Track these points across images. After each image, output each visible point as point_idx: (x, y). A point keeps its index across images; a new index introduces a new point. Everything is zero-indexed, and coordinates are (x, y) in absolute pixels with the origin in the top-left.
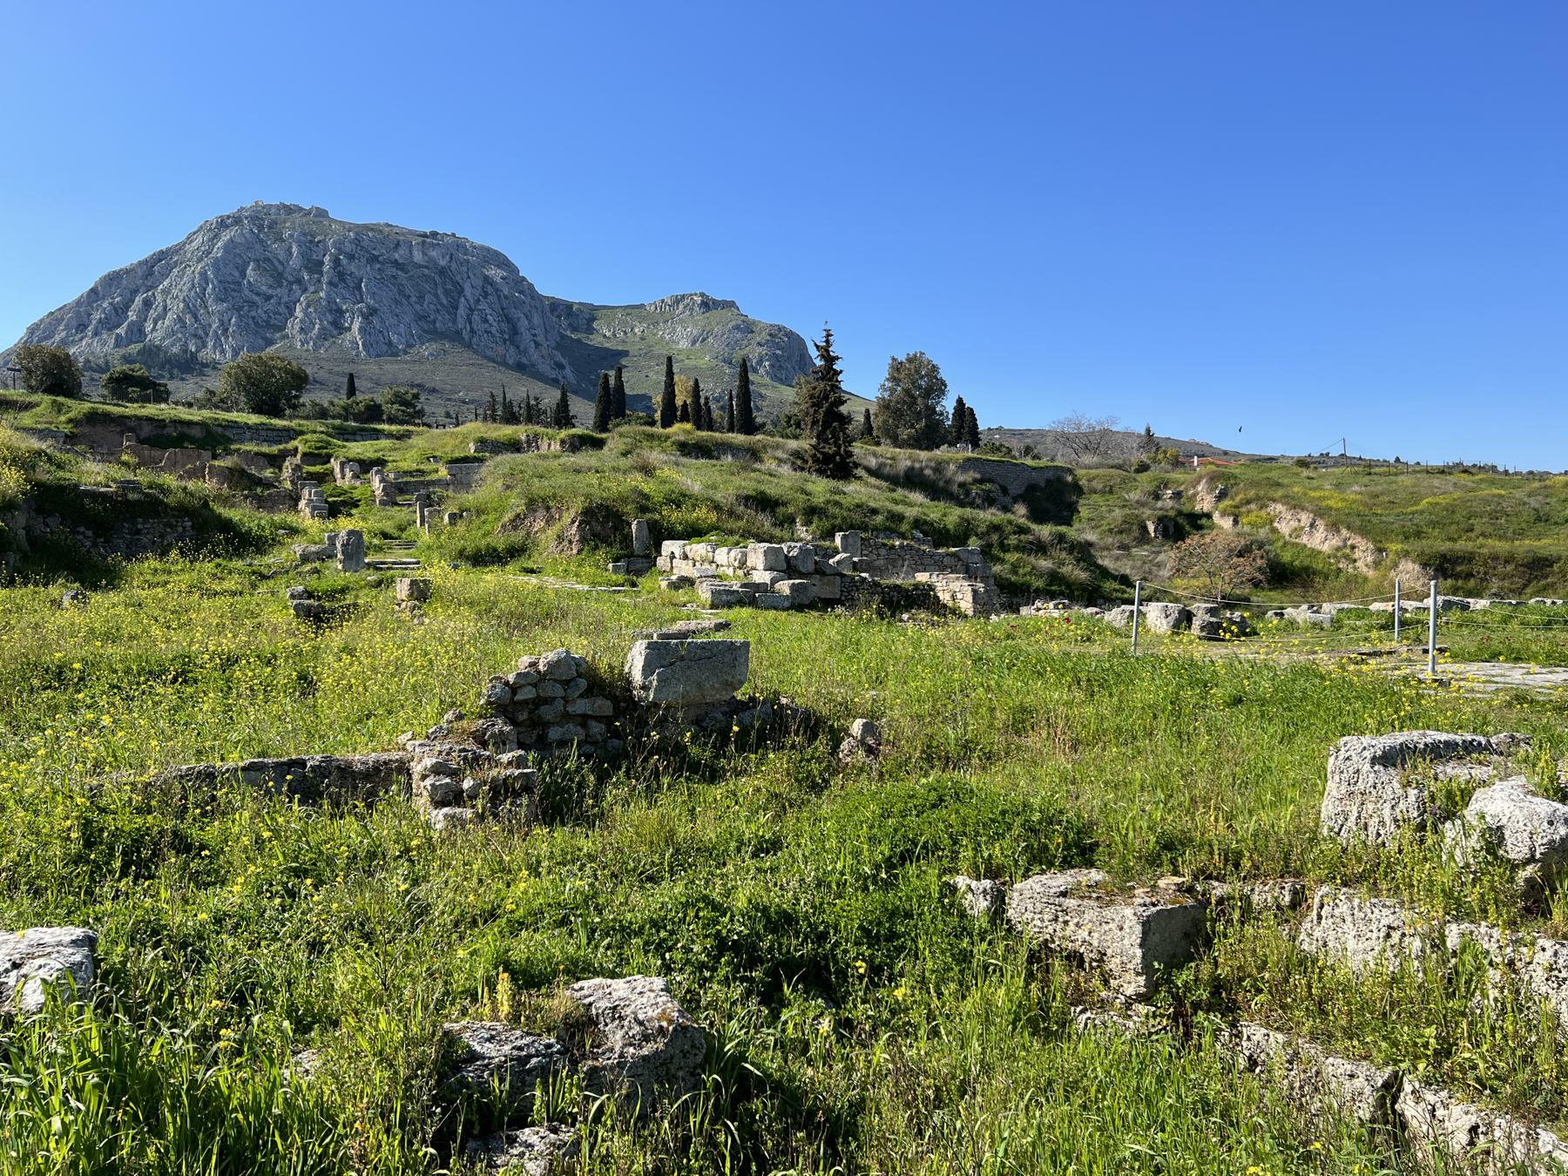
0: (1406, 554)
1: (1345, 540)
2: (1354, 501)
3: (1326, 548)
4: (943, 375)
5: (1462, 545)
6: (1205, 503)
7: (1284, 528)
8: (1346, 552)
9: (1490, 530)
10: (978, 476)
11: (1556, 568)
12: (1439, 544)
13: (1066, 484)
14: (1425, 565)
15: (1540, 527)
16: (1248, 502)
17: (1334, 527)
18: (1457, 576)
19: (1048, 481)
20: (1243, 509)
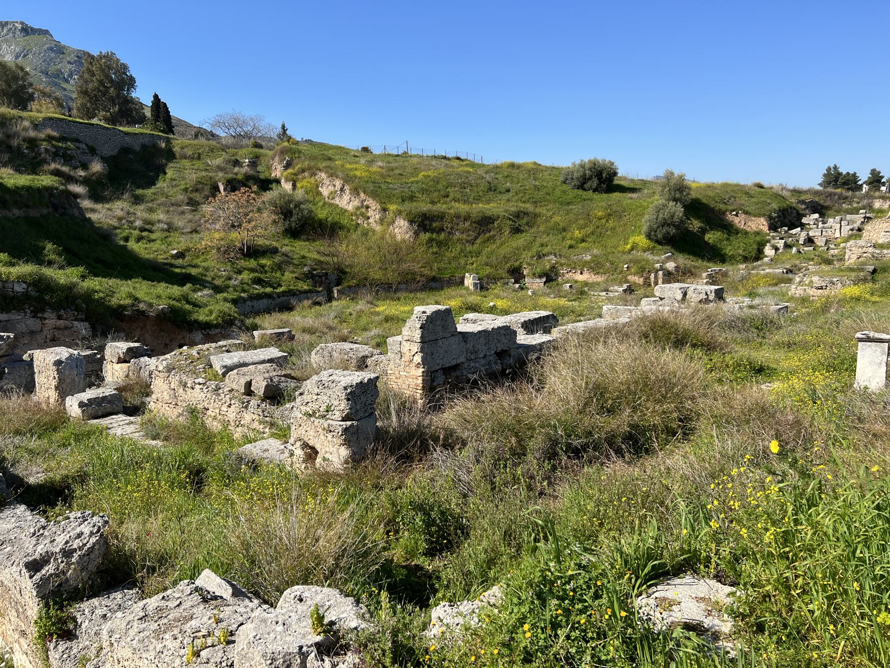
0: (400, 213)
1: (363, 201)
2: (375, 173)
3: (350, 208)
4: (133, 72)
5: (440, 207)
6: (277, 171)
7: (325, 191)
8: (362, 211)
9: (459, 196)
10: (55, 134)
11: (495, 225)
12: (424, 206)
13: (160, 150)
14: (411, 222)
16: (303, 171)
17: (355, 191)
18: (432, 231)
19: (144, 147)
20: (300, 177)
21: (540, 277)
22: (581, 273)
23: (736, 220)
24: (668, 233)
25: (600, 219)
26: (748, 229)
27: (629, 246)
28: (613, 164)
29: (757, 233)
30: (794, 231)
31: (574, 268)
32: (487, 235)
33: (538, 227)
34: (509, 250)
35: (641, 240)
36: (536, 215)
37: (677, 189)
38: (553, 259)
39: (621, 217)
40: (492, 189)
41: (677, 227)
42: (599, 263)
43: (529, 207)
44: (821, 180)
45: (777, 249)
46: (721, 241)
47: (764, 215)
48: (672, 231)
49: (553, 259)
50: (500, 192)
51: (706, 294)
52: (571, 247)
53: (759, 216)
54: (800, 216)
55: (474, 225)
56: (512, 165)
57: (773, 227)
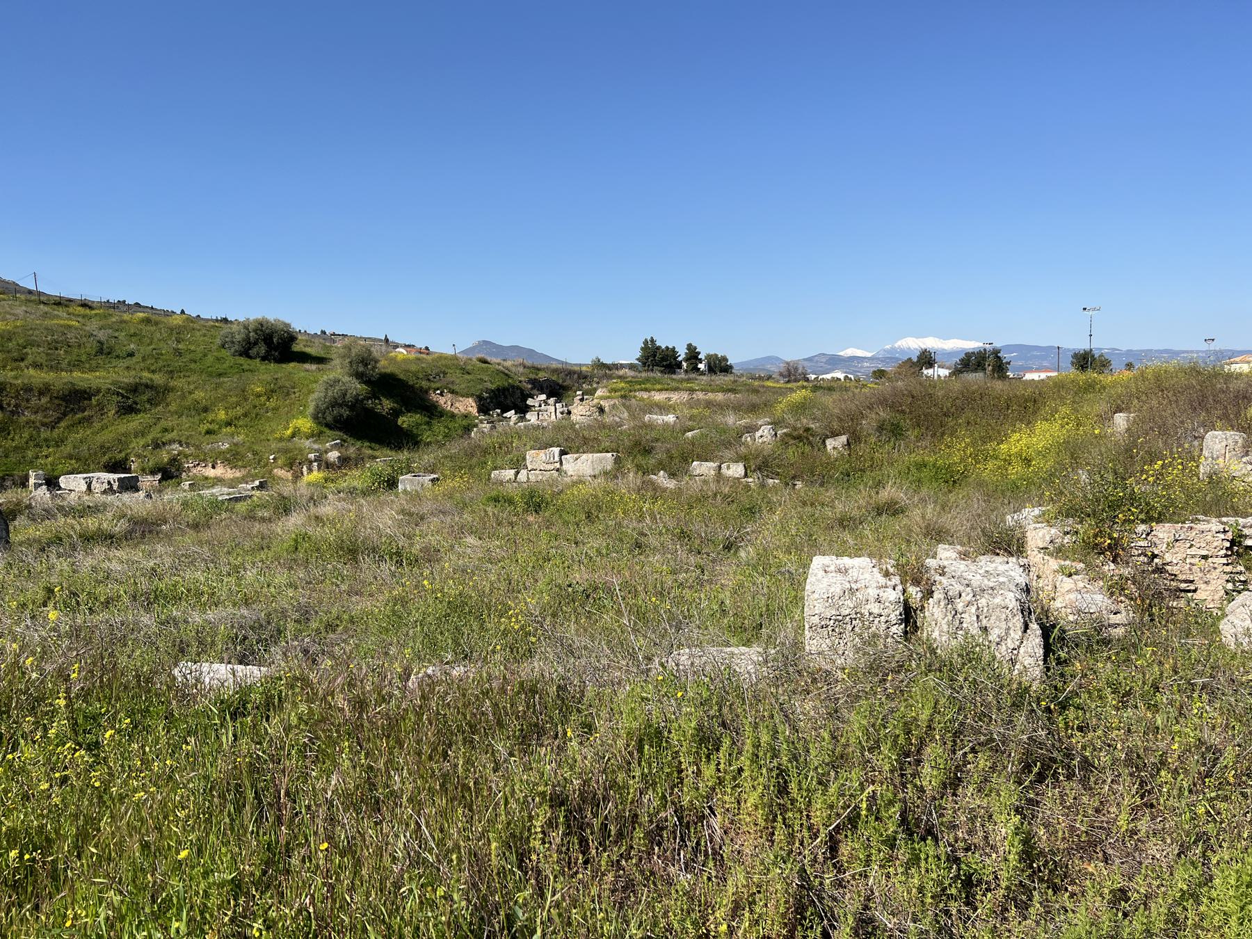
9: (42, 359)
11: (94, 401)
15: (100, 359)
21: (153, 473)
22: (213, 467)
23: (442, 400)
24: (341, 416)
25: (259, 396)
26: (456, 411)
27: (289, 432)
28: (289, 325)
30: (508, 415)
31: (204, 460)
32: (79, 416)
33: (167, 405)
34: (112, 435)
35: (305, 423)
36: (167, 389)
37: (364, 363)
38: (176, 448)
39: (288, 394)
40: (104, 351)
41: (352, 408)
42: (237, 453)
43: (158, 379)
44: (638, 355)
46: (418, 425)
47: (472, 395)
48: (346, 413)
49: (176, 448)
50: (118, 357)
51: (109, 483)
52: (209, 432)
53: (467, 396)
54: (525, 396)
55: (57, 402)
57: (484, 409)
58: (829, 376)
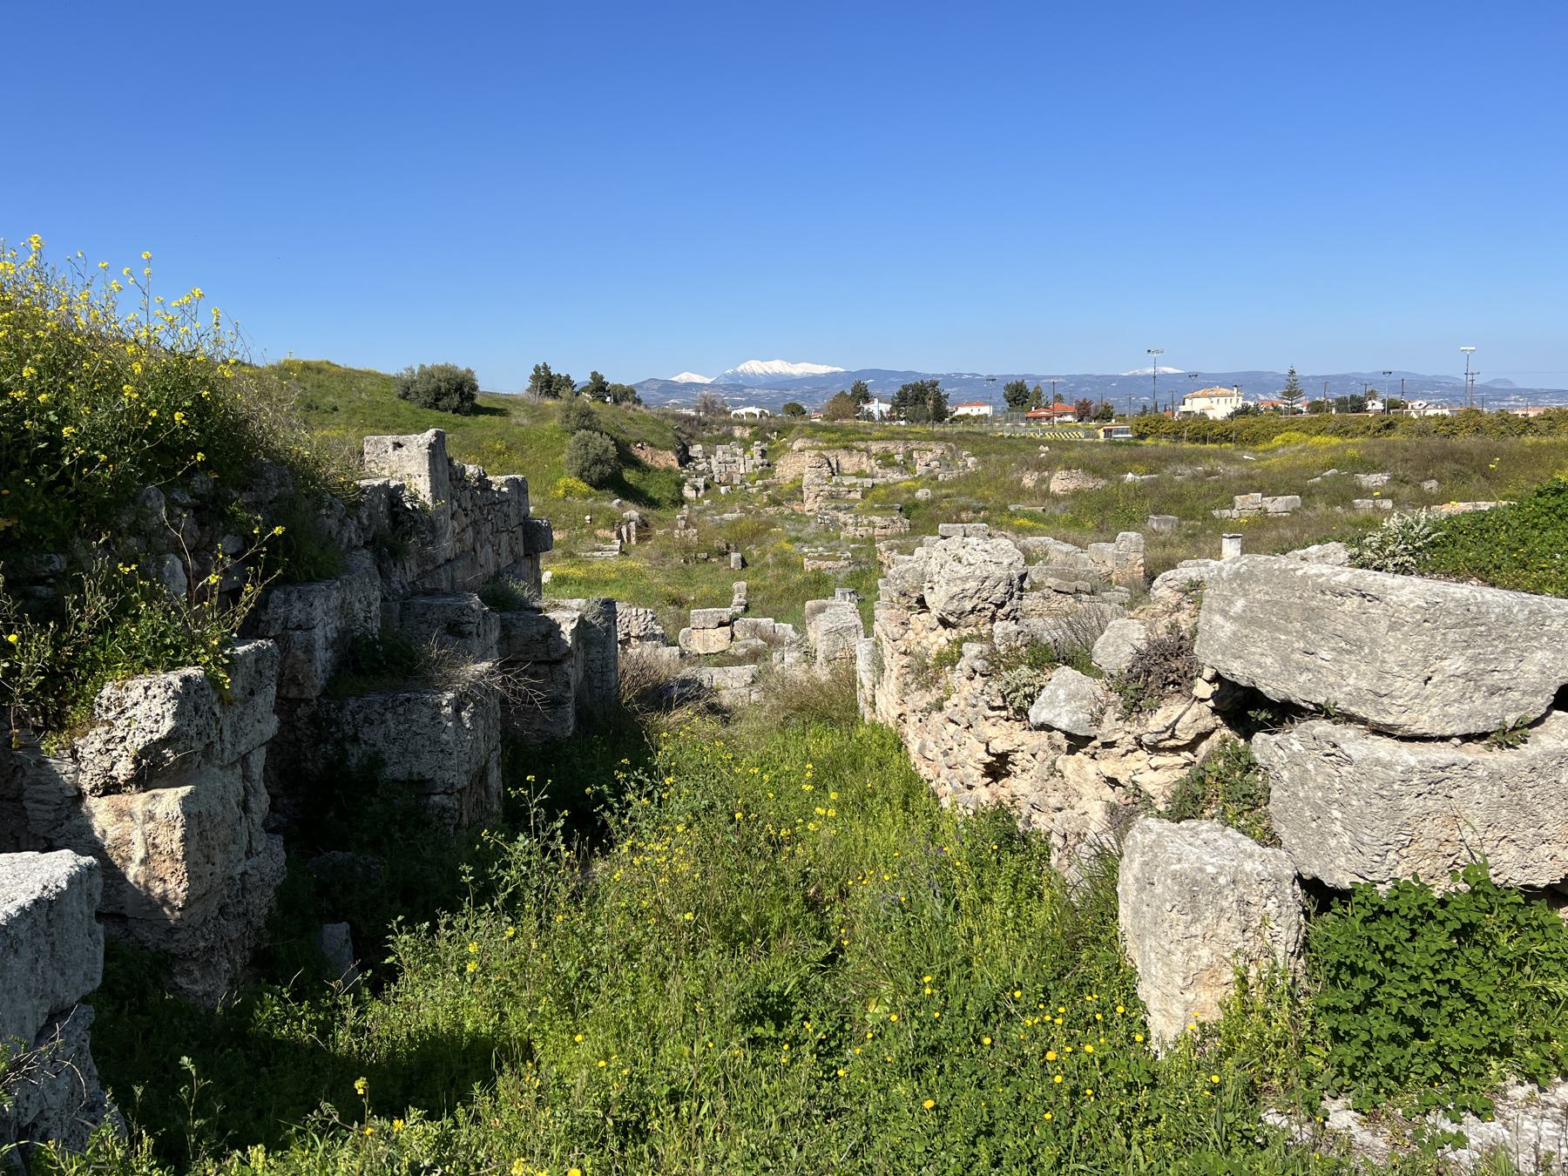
29: (669, 470)
44: (528, 384)
45: (697, 490)
53: (666, 449)
56: (307, 367)
58: (742, 411)
